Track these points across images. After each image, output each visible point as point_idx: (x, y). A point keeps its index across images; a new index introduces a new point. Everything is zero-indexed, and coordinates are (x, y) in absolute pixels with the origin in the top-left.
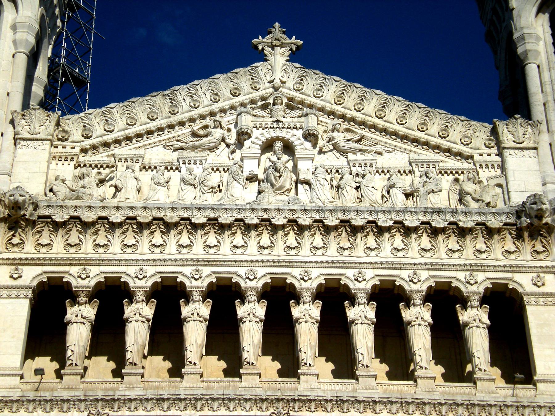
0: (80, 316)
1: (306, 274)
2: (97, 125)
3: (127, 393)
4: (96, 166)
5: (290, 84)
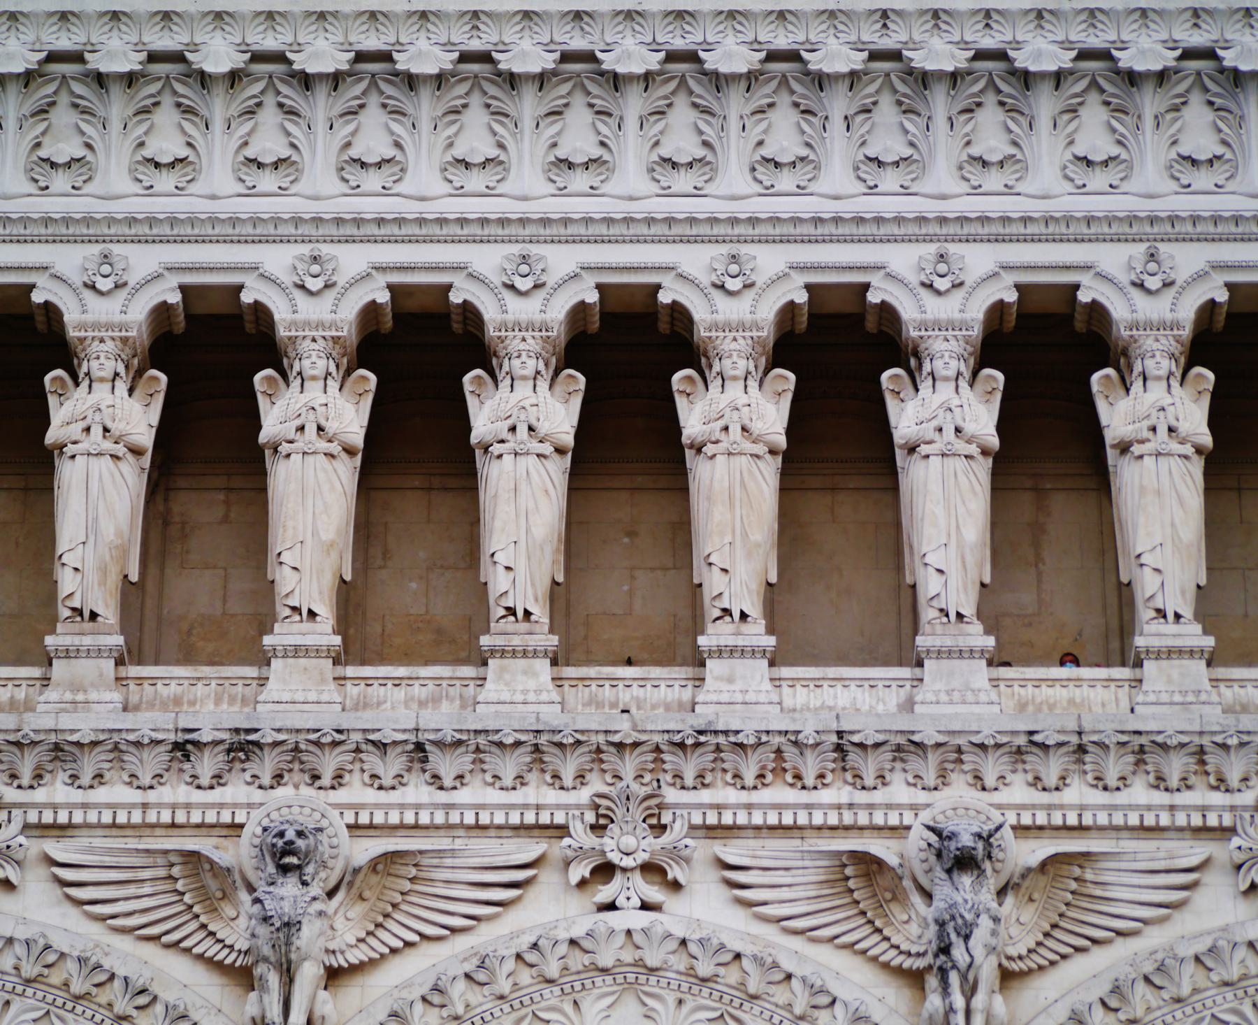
1: (734, 269)
3: (66, 722)
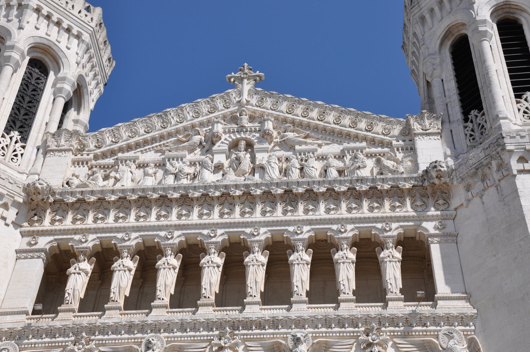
0: (77, 269)
2: (107, 139)
3: (106, 321)
4: (104, 167)
5: (254, 101)
